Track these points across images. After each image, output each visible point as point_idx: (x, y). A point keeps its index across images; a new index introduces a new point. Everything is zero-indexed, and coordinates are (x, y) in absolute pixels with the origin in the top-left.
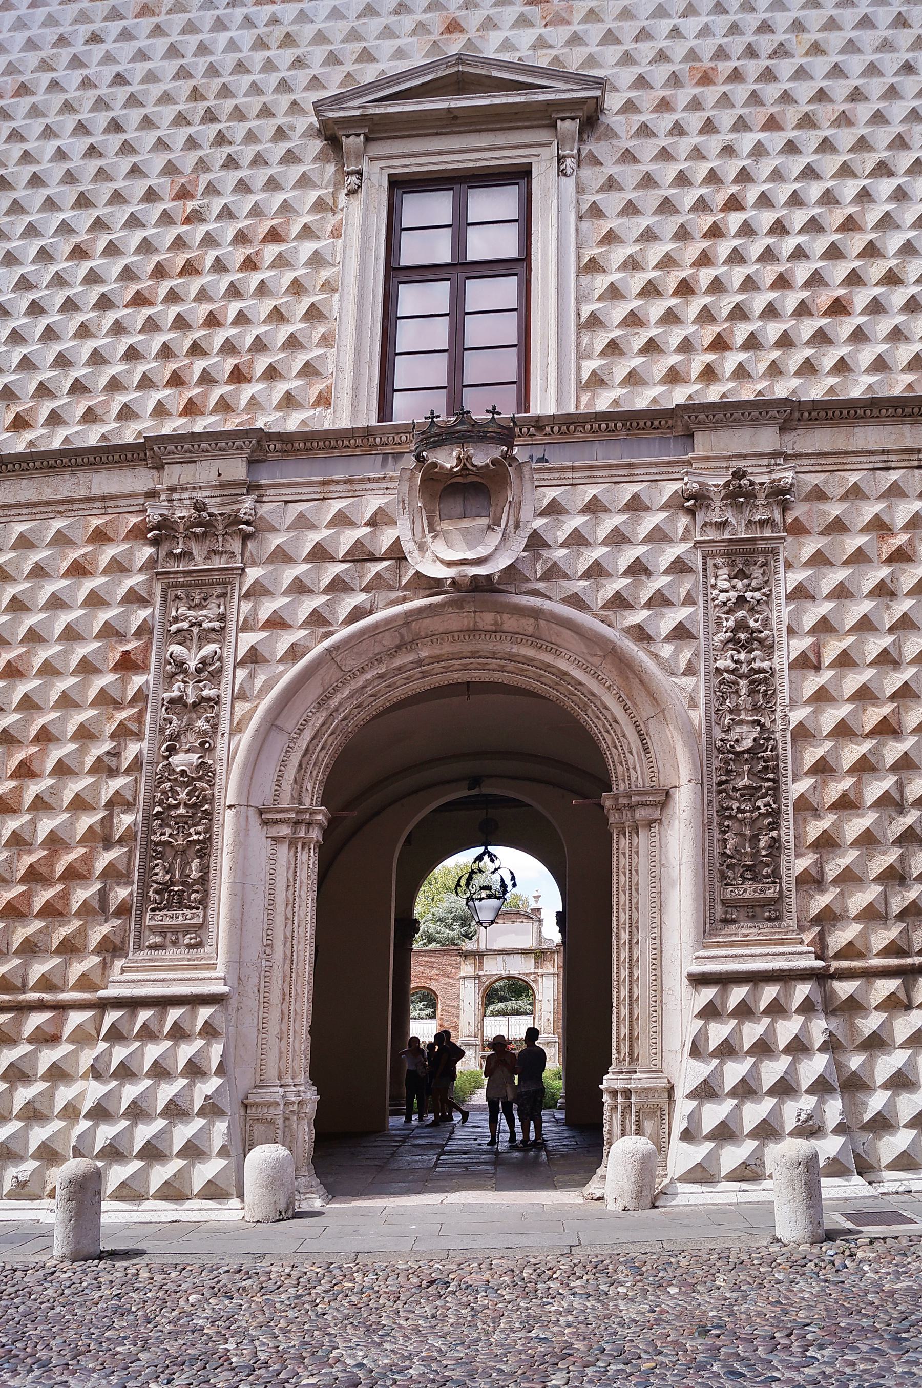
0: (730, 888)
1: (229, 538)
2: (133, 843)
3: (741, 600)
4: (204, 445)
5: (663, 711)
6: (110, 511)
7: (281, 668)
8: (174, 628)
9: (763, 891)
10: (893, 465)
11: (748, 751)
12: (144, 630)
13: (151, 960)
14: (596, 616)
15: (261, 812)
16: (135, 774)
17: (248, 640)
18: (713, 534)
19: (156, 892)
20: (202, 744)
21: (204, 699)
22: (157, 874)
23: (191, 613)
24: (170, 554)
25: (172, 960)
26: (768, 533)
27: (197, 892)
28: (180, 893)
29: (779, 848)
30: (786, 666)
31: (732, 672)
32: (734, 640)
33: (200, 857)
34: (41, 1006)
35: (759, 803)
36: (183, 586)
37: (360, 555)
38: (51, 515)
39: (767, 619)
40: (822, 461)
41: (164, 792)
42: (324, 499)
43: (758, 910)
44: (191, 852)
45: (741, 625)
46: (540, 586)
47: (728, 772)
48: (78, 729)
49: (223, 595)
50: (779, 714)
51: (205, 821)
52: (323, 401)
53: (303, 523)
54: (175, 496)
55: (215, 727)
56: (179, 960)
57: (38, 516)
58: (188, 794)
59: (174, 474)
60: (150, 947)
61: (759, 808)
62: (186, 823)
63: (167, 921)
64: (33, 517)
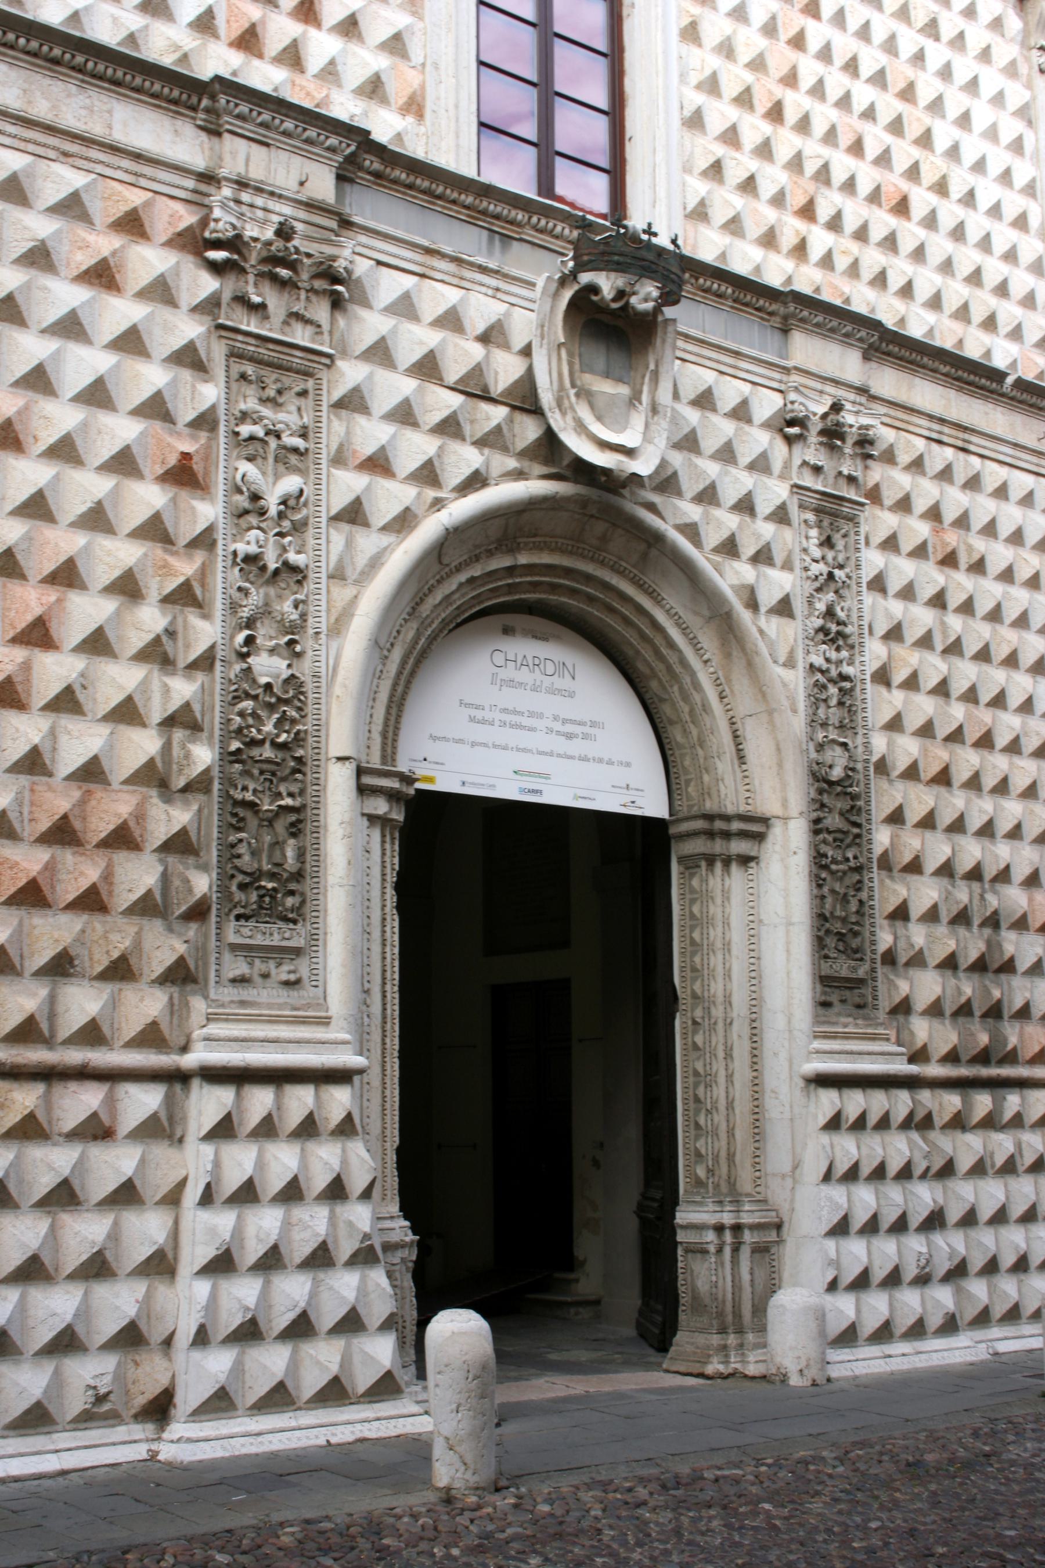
0: (830, 962)
1: (314, 298)
2: (202, 797)
3: (831, 576)
4: (289, 125)
5: (770, 712)
6: (143, 182)
7: (386, 539)
8: (245, 430)
9: (854, 969)
10: (945, 439)
11: (838, 783)
12: (205, 421)
13: (243, 1003)
14: (707, 558)
15: (360, 772)
16: (200, 677)
17: (347, 484)
18: (808, 480)
19: (242, 887)
20: (291, 643)
21: (290, 568)
22: (239, 856)
23: (266, 412)
24: (241, 300)
25: (270, 1006)
26: (852, 495)
27: (292, 893)
28: (273, 893)
29: (863, 915)
30: (868, 677)
31: (822, 672)
32: (823, 630)
33: (294, 835)
34: (84, 1074)
35: (850, 855)
36: (251, 359)
37: (475, 388)
38: (52, 154)
39: (849, 610)
40: (892, 412)
41: (242, 714)
42: (422, 276)
43: (847, 993)
44: (280, 826)
45: (830, 613)
46: (656, 498)
47: (823, 806)
48: (120, 578)
49: (303, 394)
50: (860, 740)
51: (298, 776)
52: (414, 107)
53: (405, 307)
54: (245, 197)
55: (303, 616)
56: (280, 1006)
57: (31, 148)
58: (276, 726)
59: (238, 156)
60: (234, 981)
61: (847, 860)
62: (274, 774)
63: (259, 940)
64: (22, 145)
